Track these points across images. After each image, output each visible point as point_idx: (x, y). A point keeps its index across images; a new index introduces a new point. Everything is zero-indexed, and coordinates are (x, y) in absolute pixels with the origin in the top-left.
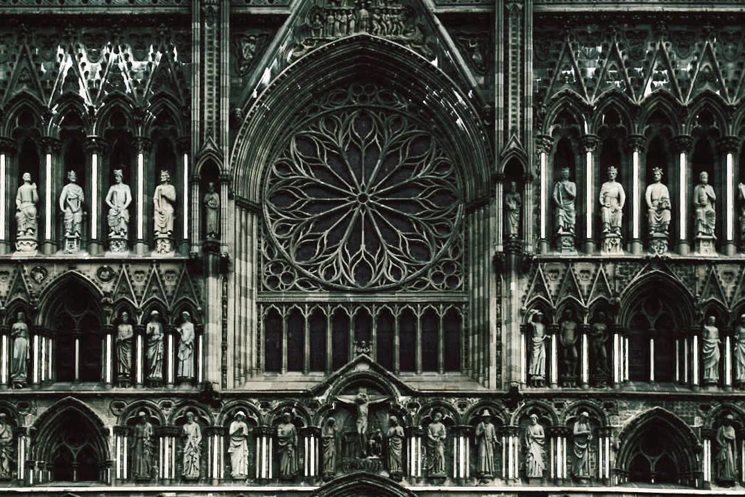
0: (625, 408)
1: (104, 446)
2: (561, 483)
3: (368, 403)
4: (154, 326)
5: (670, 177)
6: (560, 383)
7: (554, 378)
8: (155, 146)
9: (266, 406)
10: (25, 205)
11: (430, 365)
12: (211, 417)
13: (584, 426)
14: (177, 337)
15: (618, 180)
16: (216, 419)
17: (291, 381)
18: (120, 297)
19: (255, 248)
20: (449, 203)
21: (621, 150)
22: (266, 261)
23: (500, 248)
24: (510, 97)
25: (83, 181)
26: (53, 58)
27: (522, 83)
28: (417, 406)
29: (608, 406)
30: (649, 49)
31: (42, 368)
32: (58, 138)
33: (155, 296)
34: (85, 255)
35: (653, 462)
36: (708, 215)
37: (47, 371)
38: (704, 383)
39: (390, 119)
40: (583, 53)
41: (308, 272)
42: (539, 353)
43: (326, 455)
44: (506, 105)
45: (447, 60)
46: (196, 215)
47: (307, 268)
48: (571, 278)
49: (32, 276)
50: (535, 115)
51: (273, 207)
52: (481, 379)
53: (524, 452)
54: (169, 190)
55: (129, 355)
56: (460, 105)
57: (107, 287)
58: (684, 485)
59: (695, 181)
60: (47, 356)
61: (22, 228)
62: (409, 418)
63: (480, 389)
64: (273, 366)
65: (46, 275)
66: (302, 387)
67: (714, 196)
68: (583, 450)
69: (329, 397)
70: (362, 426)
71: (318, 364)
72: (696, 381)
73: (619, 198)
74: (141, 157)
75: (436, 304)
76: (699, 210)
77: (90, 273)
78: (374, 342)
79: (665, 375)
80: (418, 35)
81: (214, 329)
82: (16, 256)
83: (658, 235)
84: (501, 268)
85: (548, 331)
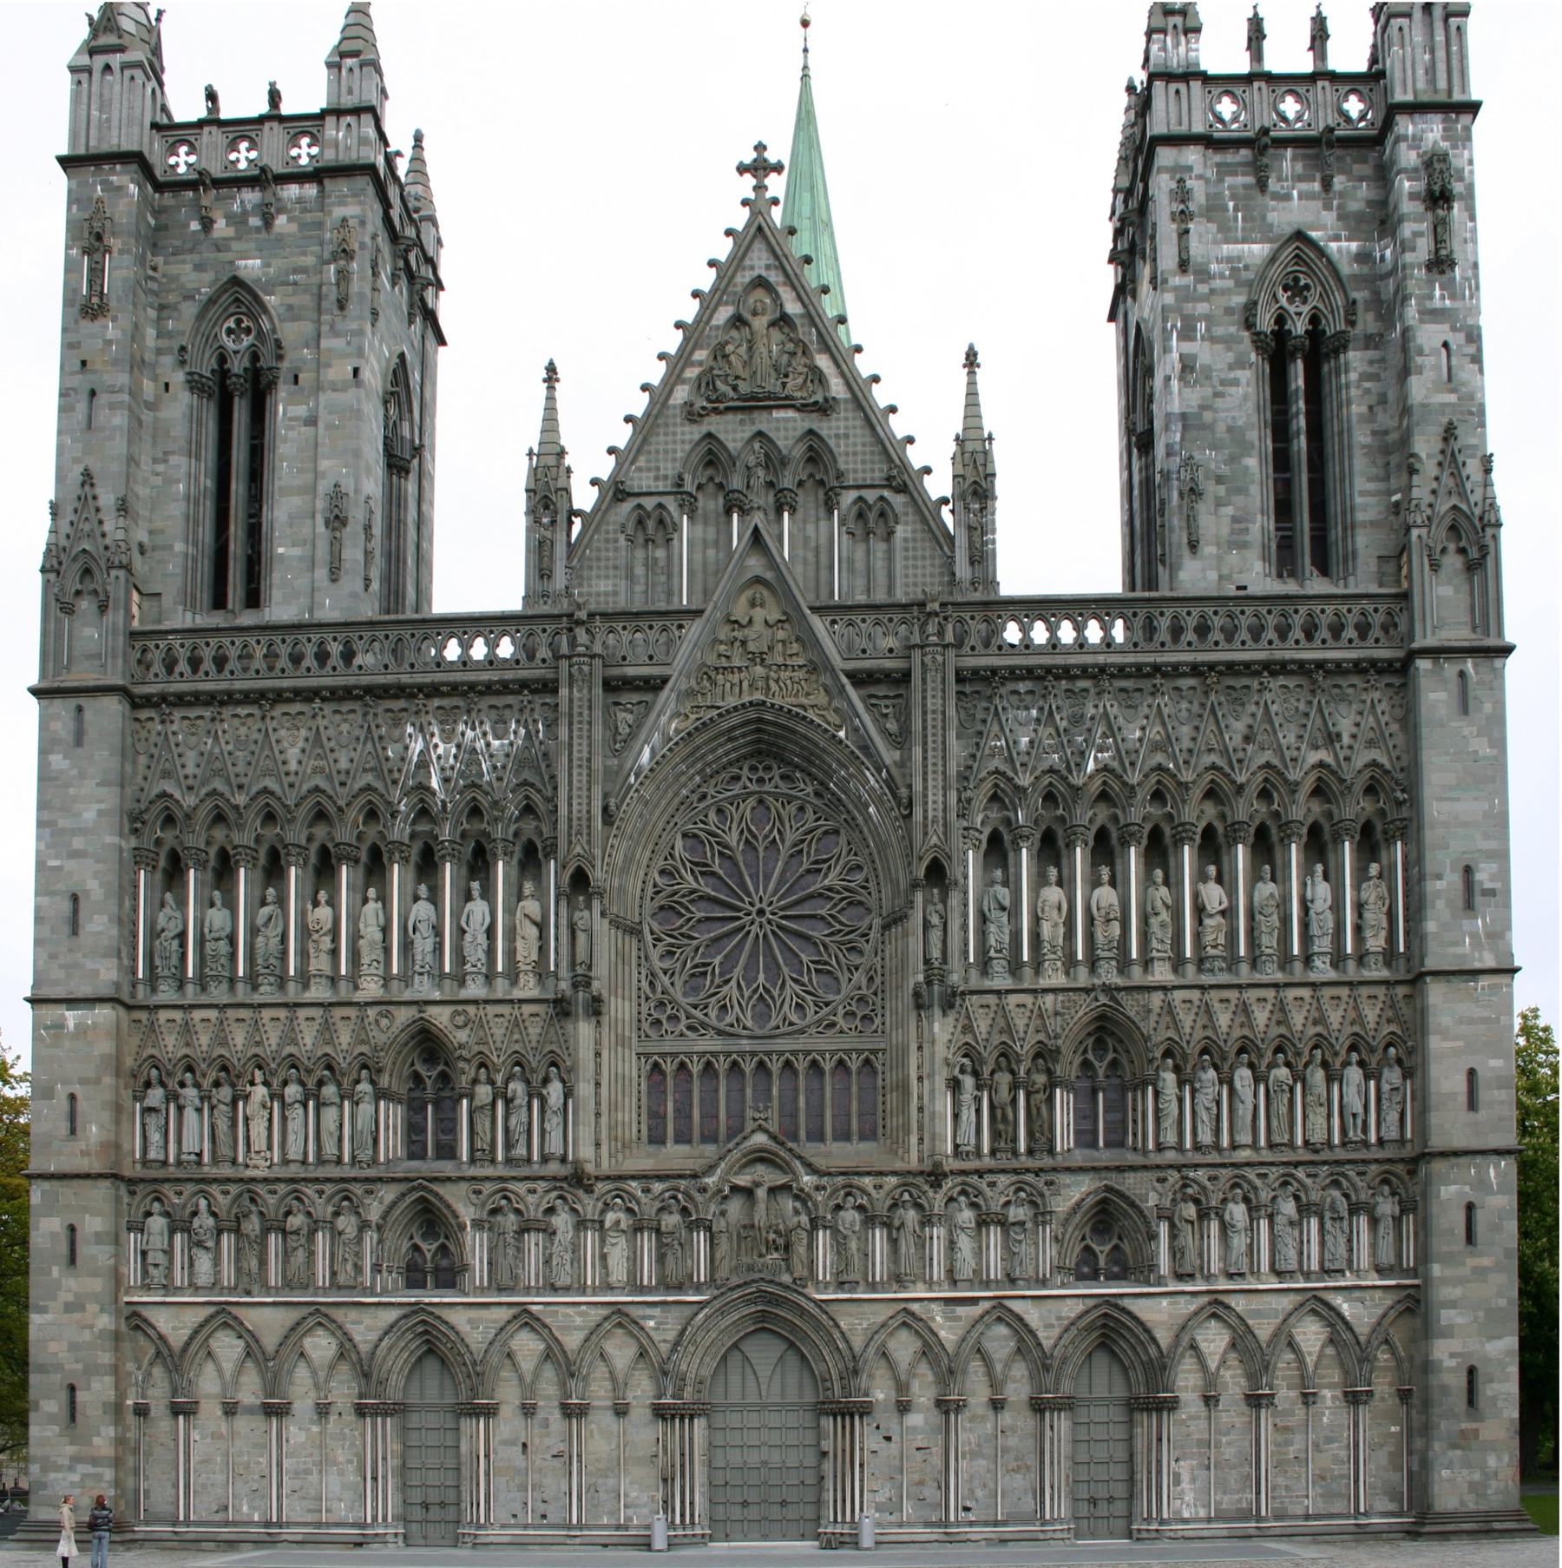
0: (1069, 1186)
1: (460, 1245)
2: (993, 1285)
3: (766, 1187)
4: (516, 1087)
5: (1119, 876)
6: (993, 1152)
7: (986, 1150)
8: (518, 849)
9: (647, 1191)
10: (370, 929)
11: (844, 1135)
12: (583, 1206)
13: (1021, 1211)
14: (543, 1101)
15: (1060, 883)
16: (589, 1209)
17: (676, 1155)
18: (476, 1048)
19: (635, 982)
20: (861, 918)
21: (1061, 843)
22: (647, 999)
23: (921, 978)
24: (930, 777)
25: (435, 898)
26: (400, 739)
27: (944, 758)
28: (824, 1188)
29: (1049, 1184)
30: (1091, 711)
31: (391, 1143)
32: (406, 841)
33: (517, 1047)
34: (437, 996)
35: (1102, 1250)
36: (1163, 925)
37: (395, 1147)
38: (1160, 1148)
39: (792, 808)
40: (1016, 718)
41: (697, 1013)
42: (968, 1115)
43: (718, 1255)
44: (925, 788)
45: (856, 730)
46: (564, 939)
47: (695, 1007)
48: (1005, 1017)
49: (377, 1021)
50: (959, 800)
51: (655, 927)
52: (900, 1151)
53: (952, 1245)
54: (531, 907)
55: (488, 1125)
56: (872, 788)
57: (462, 1036)
58: (1138, 1282)
59: (1147, 880)
60: (395, 1127)
61: (365, 960)
62: (815, 1204)
63: (899, 1165)
64: (657, 1139)
65: (392, 1022)
66: (690, 1165)
67: (1169, 902)
68: (1020, 1242)
69: (723, 1180)
70: (760, 1216)
71: (710, 1137)
72: (1151, 1146)
73: (1059, 909)
74: (500, 864)
75: (847, 1052)
76: (1153, 921)
77: (441, 1017)
78: (776, 1103)
79: (1115, 1142)
80: (822, 699)
81: (584, 1089)
82: (359, 996)
83: (1106, 954)
84: (920, 1003)
85: (979, 1087)
